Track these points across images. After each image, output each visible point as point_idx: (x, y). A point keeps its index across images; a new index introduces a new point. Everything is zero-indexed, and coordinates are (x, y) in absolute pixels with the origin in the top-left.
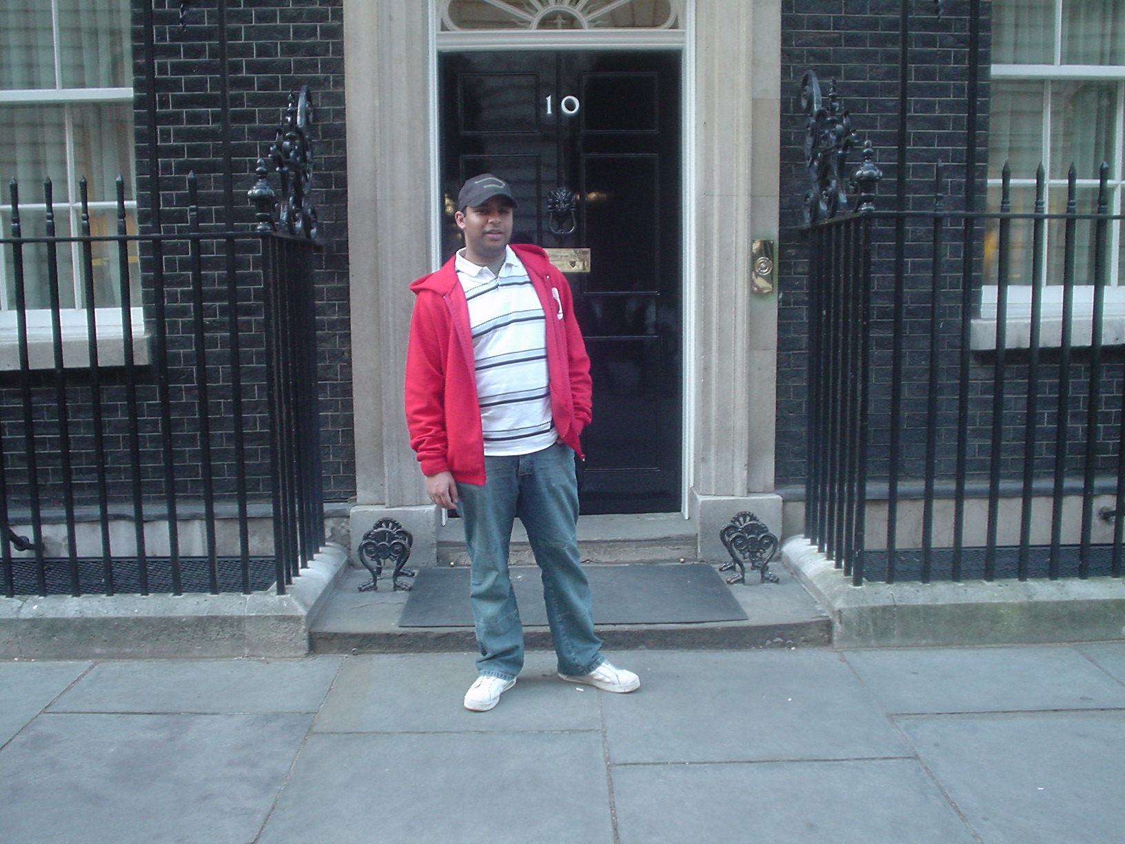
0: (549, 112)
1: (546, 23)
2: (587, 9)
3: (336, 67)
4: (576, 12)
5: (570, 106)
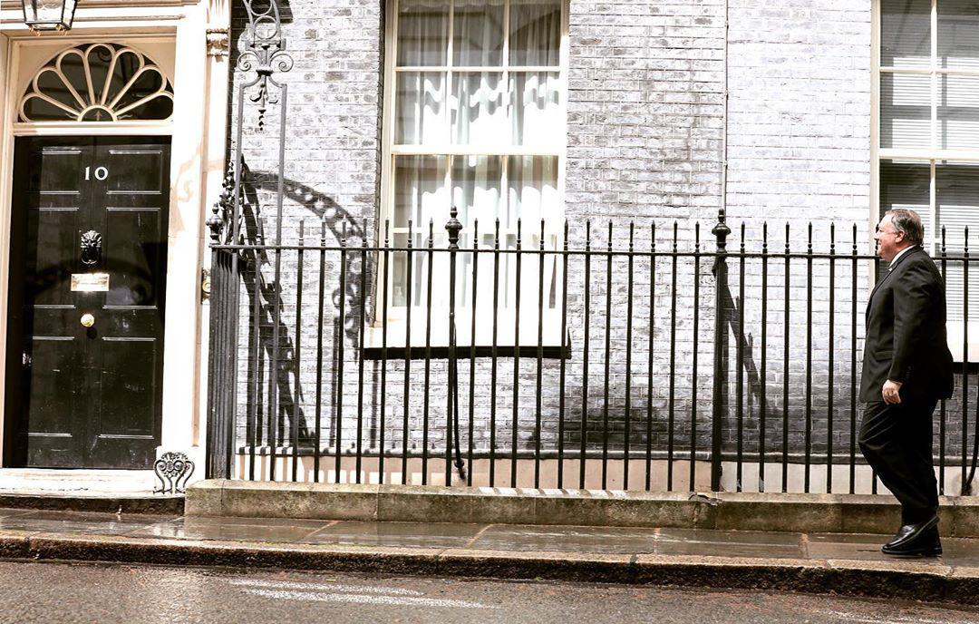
0: (87, 178)
1: (90, 117)
4: (109, 109)
5: (101, 173)
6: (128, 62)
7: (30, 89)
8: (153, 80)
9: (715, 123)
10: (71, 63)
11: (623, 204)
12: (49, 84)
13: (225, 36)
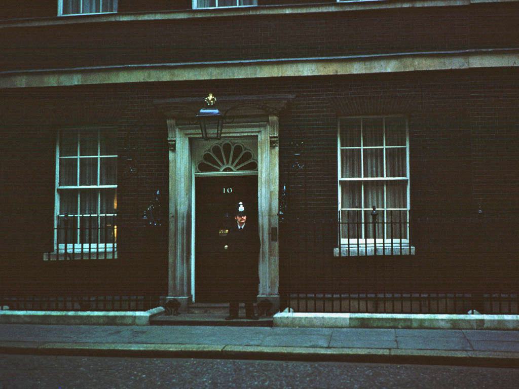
1: (225, 170)
4: (232, 168)
6: (238, 149)
8: (248, 156)
10: (216, 150)
12: (207, 157)
13: (278, 139)
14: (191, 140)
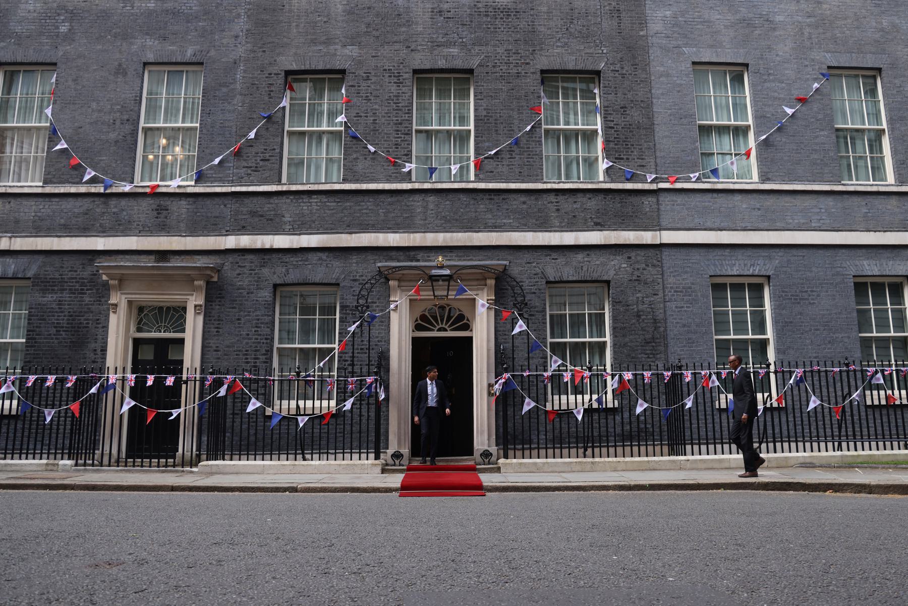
1: (439, 330)
2: (449, 326)
3: (388, 342)
7: (417, 320)
9: (662, 329)
11: (633, 358)
14: (410, 300)
